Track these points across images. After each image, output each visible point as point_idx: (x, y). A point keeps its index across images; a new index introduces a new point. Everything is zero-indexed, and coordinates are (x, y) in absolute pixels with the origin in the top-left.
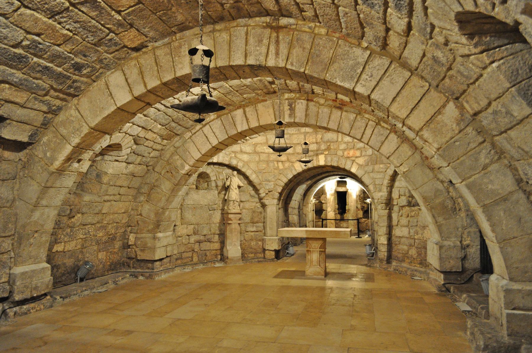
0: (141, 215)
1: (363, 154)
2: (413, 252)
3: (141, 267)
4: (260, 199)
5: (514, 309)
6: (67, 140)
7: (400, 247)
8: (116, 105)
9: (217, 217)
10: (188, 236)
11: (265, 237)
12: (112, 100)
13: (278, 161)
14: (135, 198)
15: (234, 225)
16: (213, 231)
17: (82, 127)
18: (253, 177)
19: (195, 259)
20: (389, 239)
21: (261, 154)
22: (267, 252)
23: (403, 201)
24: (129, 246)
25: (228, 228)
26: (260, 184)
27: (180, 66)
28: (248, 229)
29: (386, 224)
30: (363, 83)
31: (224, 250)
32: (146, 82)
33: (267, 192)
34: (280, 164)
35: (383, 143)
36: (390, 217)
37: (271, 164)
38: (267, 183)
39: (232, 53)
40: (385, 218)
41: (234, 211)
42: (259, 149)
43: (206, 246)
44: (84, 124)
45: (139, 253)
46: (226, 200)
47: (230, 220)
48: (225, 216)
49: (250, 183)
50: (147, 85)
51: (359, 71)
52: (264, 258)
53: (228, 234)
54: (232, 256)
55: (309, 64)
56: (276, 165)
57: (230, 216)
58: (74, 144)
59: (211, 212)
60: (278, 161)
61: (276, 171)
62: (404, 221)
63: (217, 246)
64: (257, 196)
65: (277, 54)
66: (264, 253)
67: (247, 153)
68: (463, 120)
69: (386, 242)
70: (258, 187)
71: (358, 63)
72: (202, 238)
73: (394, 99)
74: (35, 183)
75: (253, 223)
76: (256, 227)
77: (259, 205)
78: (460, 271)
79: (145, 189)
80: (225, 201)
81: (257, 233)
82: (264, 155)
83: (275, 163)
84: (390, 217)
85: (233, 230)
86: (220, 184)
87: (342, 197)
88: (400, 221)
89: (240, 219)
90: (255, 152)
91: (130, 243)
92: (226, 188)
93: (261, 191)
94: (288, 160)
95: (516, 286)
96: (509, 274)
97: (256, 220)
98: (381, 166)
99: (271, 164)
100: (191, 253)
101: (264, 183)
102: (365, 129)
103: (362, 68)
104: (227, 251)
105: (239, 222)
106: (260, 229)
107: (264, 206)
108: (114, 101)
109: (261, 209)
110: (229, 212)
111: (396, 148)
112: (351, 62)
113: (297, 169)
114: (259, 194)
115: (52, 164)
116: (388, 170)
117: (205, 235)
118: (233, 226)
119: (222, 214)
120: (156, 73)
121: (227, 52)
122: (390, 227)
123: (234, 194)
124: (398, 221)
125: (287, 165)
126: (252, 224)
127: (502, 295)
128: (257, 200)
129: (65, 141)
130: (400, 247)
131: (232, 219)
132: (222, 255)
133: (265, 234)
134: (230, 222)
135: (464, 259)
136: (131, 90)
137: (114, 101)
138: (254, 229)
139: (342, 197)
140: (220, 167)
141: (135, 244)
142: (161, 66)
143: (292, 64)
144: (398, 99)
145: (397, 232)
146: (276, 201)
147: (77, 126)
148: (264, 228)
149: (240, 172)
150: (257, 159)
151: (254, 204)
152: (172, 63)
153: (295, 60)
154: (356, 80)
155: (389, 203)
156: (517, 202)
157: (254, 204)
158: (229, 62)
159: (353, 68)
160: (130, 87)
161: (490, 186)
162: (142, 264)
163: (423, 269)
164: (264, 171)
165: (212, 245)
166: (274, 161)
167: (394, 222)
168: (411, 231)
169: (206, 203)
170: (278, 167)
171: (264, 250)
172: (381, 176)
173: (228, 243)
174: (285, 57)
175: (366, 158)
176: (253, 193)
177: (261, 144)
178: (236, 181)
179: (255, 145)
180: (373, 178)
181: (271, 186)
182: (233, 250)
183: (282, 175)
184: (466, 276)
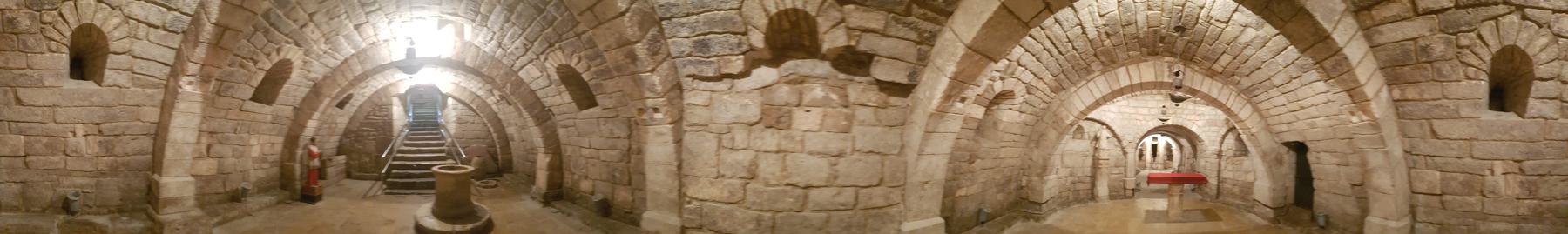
2: (1236, 190)
9: (1089, 161)
14: (1027, 144)
15: (1104, 170)
18: (1118, 131)
23: (1231, 153)
43: (1081, 186)
49: (1115, 135)
62: (1230, 167)
63: (1088, 186)
79: (1035, 137)
80: (1096, 149)
87: (1154, 147)
92: (1097, 139)
107: (1125, 153)
123: (1104, 144)
139: (1154, 147)
149: (1109, 128)
151: (1117, 152)
155: (1220, 155)
178: (1105, 133)
181: (1131, 138)
182: (1103, 189)
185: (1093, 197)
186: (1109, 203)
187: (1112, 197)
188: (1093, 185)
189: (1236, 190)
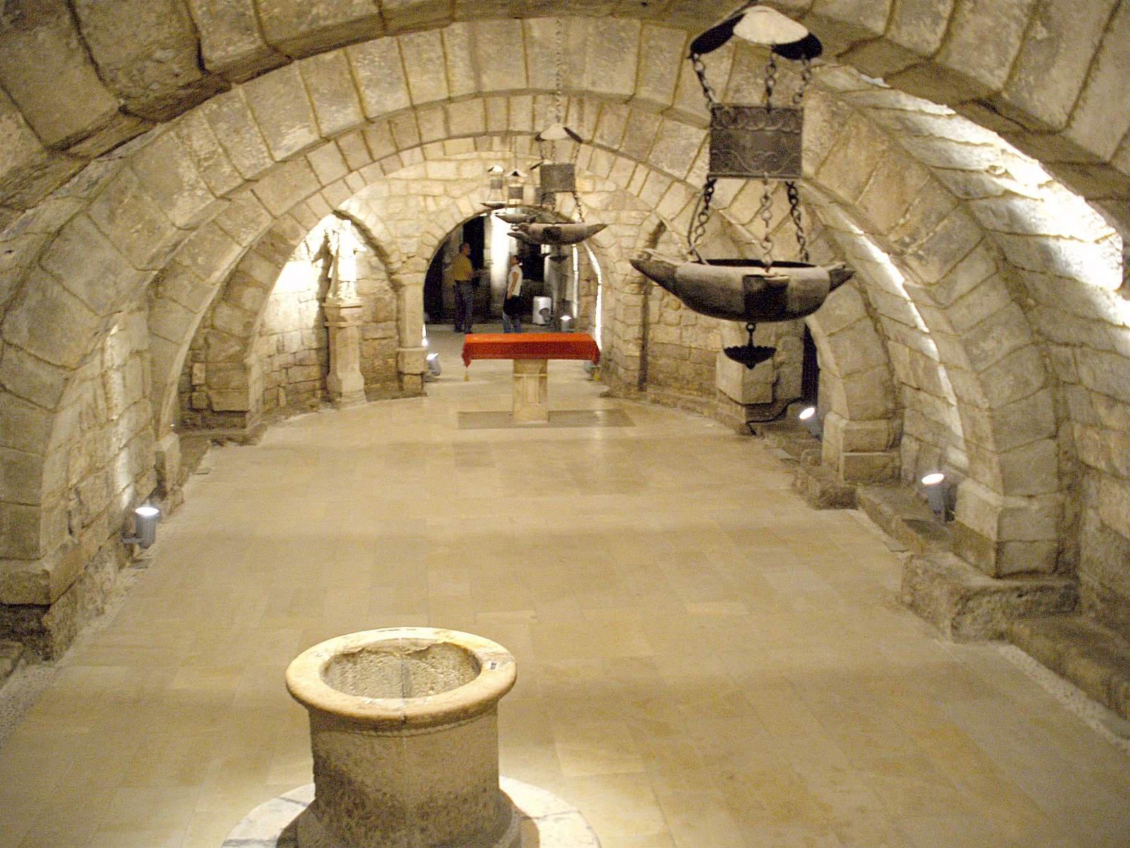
0: (212, 326)
1: (599, 187)
3: (222, 426)
4: (391, 273)
5: (852, 451)
6: (233, 237)
7: (662, 361)
8: (320, 182)
10: (270, 356)
11: (401, 350)
12: (312, 175)
13: (425, 196)
17: (259, 216)
19: (283, 401)
20: (643, 347)
22: (406, 379)
24: (193, 388)
25: (338, 336)
26: (391, 243)
27: (428, 126)
28: (369, 335)
29: (638, 320)
30: (698, 172)
31: (329, 378)
32: (372, 147)
33: (404, 259)
34: (430, 201)
35: (662, 197)
36: (645, 308)
38: (405, 240)
39: (512, 113)
40: (639, 310)
41: (348, 302)
43: (297, 374)
44: (263, 211)
45: (215, 399)
46: (329, 280)
47: (343, 319)
48: (329, 312)
50: (374, 152)
51: (693, 154)
52: (401, 388)
53: (338, 347)
54: (349, 390)
55: (626, 139)
56: (423, 204)
57: (344, 313)
58: (245, 244)
59: (303, 306)
60: (425, 196)
61: (422, 216)
63: (315, 372)
64: (382, 267)
65: (581, 119)
66: (401, 381)
68: (813, 229)
69: (638, 354)
70: (388, 250)
71: (692, 144)
72: (290, 359)
73: (735, 198)
74: (180, 307)
75: (377, 322)
76: (383, 329)
78: (770, 401)
81: (384, 342)
83: (421, 198)
84: (645, 308)
85: (350, 341)
86: (316, 247)
88: (665, 315)
89: (359, 318)
91: (196, 382)
92: (326, 255)
93: (393, 258)
94: (446, 193)
95: (856, 426)
96: (850, 411)
97: (382, 315)
98: (633, 214)
99: (412, 202)
100: (275, 390)
101: (399, 240)
102: (634, 172)
103: (696, 151)
104: (339, 381)
106: (389, 333)
107: (396, 287)
108: (316, 176)
109: (391, 294)
110: (343, 305)
111: (683, 206)
112: (683, 142)
113: (463, 210)
114: (386, 264)
115: (209, 276)
116: (646, 223)
118: (349, 332)
119: (321, 308)
120: (387, 135)
121: (504, 111)
122: (645, 325)
124: (661, 315)
125: (444, 202)
126: (375, 325)
127: (841, 436)
128: (383, 275)
129: (230, 239)
130: (662, 361)
131: (347, 318)
132: (324, 388)
133: (400, 343)
134: (343, 324)
135: (775, 385)
136: (345, 160)
137: (316, 176)
138: (379, 335)
141: (207, 384)
142: (396, 124)
143: (602, 137)
144: (740, 197)
145: (659, 334)
147: (251, 215)
148: (399, 330)
149: (357, 224)
150: (385, 194)
152: (414, 121)
153: (606, 132)
154: (688, 167)
156: (864, 331)
157: (377, 284)
158: (508, 125)
159: (685, 150)
160: (343, 155)
161: (838, 312)
162: (222, 419)
163: (704, 399)
166: (416, 194)
167: (654, 316)
168: (684, 334)
170: (426, 207)
171: (400, 375)
172: (632, 233)
173: (338, 366)
174: (591, 126)
175: (604, 195)
176: (375, 260)
180: (615, 236)
181: (411, 247)
182: (350, 378)
183: (433, 224)
184: (778, 408)
186: (363, 405)
187: (369, 394)
188: (327, 367)
189: (687, 370)
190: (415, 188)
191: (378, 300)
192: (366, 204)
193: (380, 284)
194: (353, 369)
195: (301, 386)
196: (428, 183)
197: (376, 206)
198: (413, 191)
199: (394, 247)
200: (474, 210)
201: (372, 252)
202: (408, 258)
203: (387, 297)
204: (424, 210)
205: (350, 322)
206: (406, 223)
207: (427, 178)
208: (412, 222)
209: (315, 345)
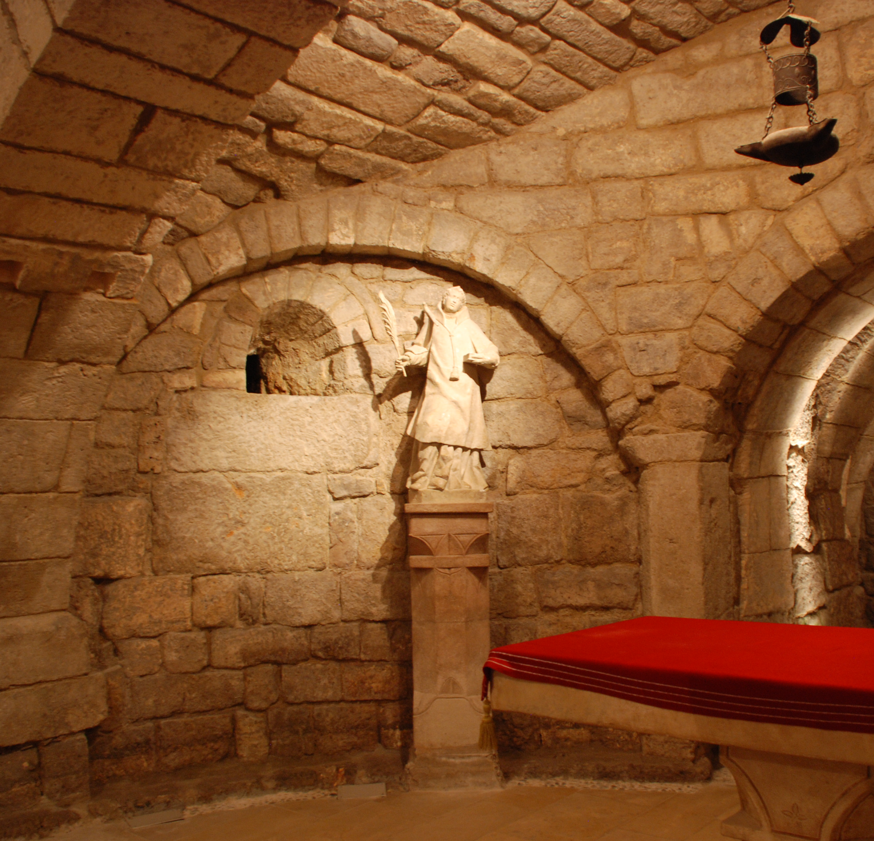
4: (616, 432)
13: (697, 215)
16: (355, 606)
21: (608, 186)
26: (604, 347)
28: (557, 597)
33: (645, 390)
34: (711, 227)
37: (661, 235)
38: (642, 340)
42: (590, 160)
43: (319, 683)
56: (690, 237)
61: (689, 272)
67: (524, 188)
70: (593, 367)
75: (582, 561)
76: (599, 585)
77: (611, 465)
82: (622, 189)
83: (685, 224)
89: (481, 543)
90: (572, 180)
93: (610, 390)
99: (661, 235)
101: (624, 341)
105: (477, 559)
113: (806, 243)
114: (602, 405)
117: (310, 626)
118: (439, 583)
125: (749, 226)
126: (576, 569)
128: (599, 438)
131: (431, 542)
138: (590, 596)
140: (391, 273)
146: (694, 442)
164: (625, 277)
165: (352, 674)
166: (675, 214)
169: (310, 465)
170: (701, 243)
176: (574, 398)
177: (602, 130)
179: (571, 140)
181: (663, 356)
183: (723, 291)
185: (385, 734)
186: (483, 788)
190: (671, 194)
191: (586, 504)
192: (518, 244)
193: (583, 457)
194: (452, 686)
195: (329, 714)
196: (705, 180)
197: (555, 251)
198: (661, 207)
199: (610, 358)
200: (839, 238)
201: (566, 378)
202: (659, 388)
203: (611, 498)
204: (695, 255)
205: (445, 556)
206: (646, 294)
207: (698, 168)
208: (662, 289)
209: (380, 610)
